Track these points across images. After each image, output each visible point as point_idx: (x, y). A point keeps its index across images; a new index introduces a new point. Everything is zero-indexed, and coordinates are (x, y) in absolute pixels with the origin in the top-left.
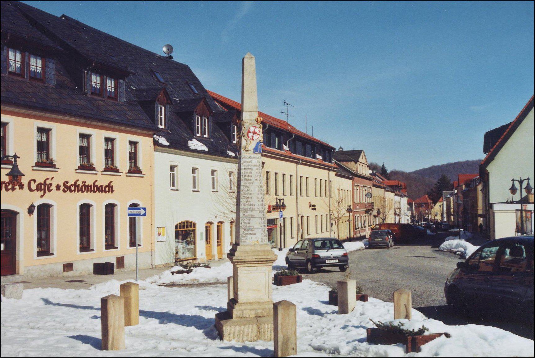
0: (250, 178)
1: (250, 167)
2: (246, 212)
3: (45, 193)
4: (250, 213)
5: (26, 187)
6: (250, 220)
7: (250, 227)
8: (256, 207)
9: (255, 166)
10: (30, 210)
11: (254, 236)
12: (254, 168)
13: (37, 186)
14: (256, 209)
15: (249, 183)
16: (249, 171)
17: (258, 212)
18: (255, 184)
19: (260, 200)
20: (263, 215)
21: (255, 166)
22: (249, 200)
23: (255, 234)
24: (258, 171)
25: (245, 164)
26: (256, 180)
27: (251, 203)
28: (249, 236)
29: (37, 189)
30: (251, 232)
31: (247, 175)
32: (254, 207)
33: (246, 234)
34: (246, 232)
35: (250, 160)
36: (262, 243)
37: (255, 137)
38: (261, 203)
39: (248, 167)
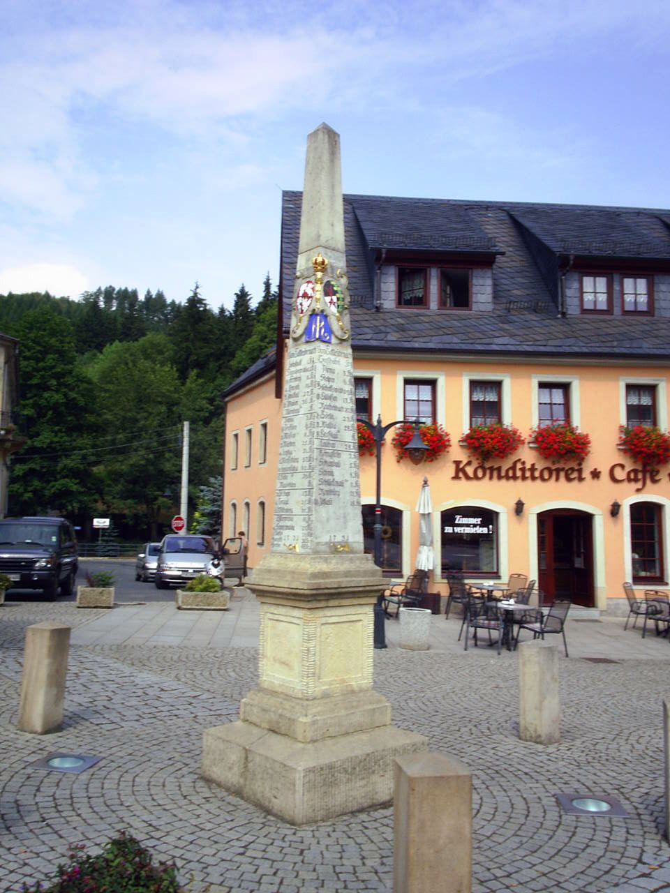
0: (295, 399)
1: (298, 375)
2: (285, 478)
3: (644, 484)
4: (289, 480)
5: (605, 476)
6: (288, 494)
7: (287, 510)
8: (299, 465)
9: (305, 370)
10: (615, 511)
11: (290, 533)
12: (303, 375)
13: (629, 473)
14: (299, 470)
15: (293, 411)
16: (294, 384)
17: (301, 475)
18: (302, 411)
19: (307, 447)
20: (310, 482)
21: (305, 370)
22: (291, 448)
23: (292, 528)
24: (309, 382)
25: (293, 369)
26: (304, 402)
27: (294, 455)
28: (286, 533)
29: (629, 480)
30: (289, 523)
31: (292, 392)
32: (295, 464)
33: (281, 527)
34: (281, 523)
35: (298, 359)
36: (303, 551)
37: (306, 303)
38: (308, 455)
39: (295, 376)
